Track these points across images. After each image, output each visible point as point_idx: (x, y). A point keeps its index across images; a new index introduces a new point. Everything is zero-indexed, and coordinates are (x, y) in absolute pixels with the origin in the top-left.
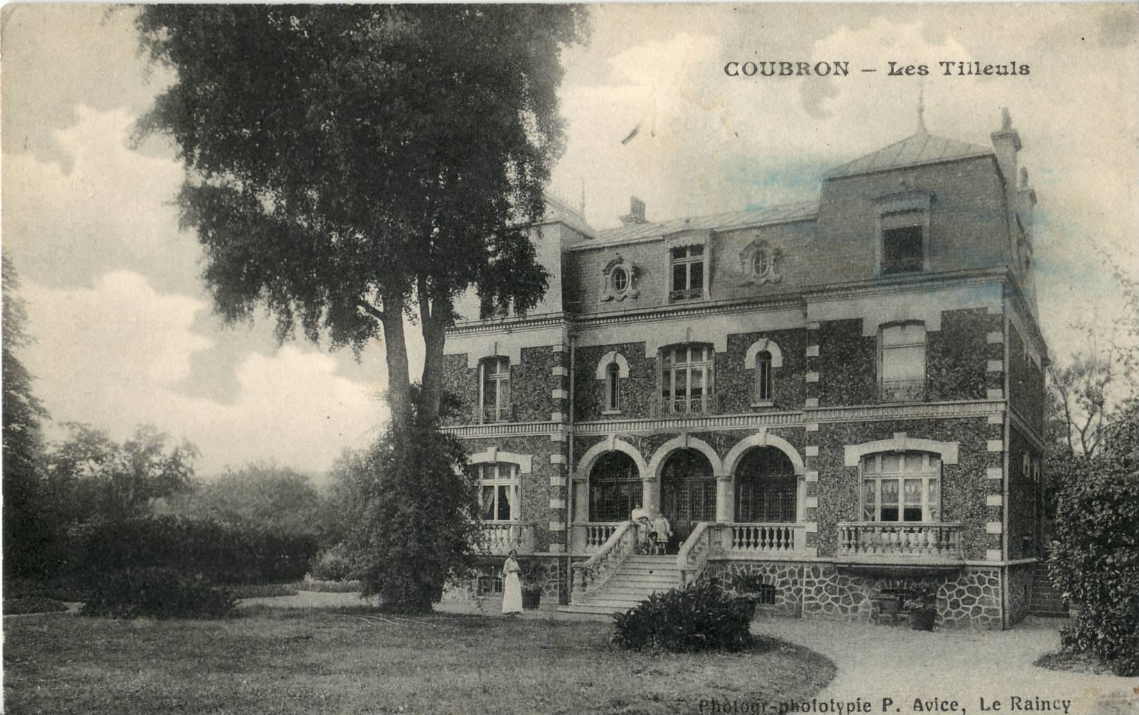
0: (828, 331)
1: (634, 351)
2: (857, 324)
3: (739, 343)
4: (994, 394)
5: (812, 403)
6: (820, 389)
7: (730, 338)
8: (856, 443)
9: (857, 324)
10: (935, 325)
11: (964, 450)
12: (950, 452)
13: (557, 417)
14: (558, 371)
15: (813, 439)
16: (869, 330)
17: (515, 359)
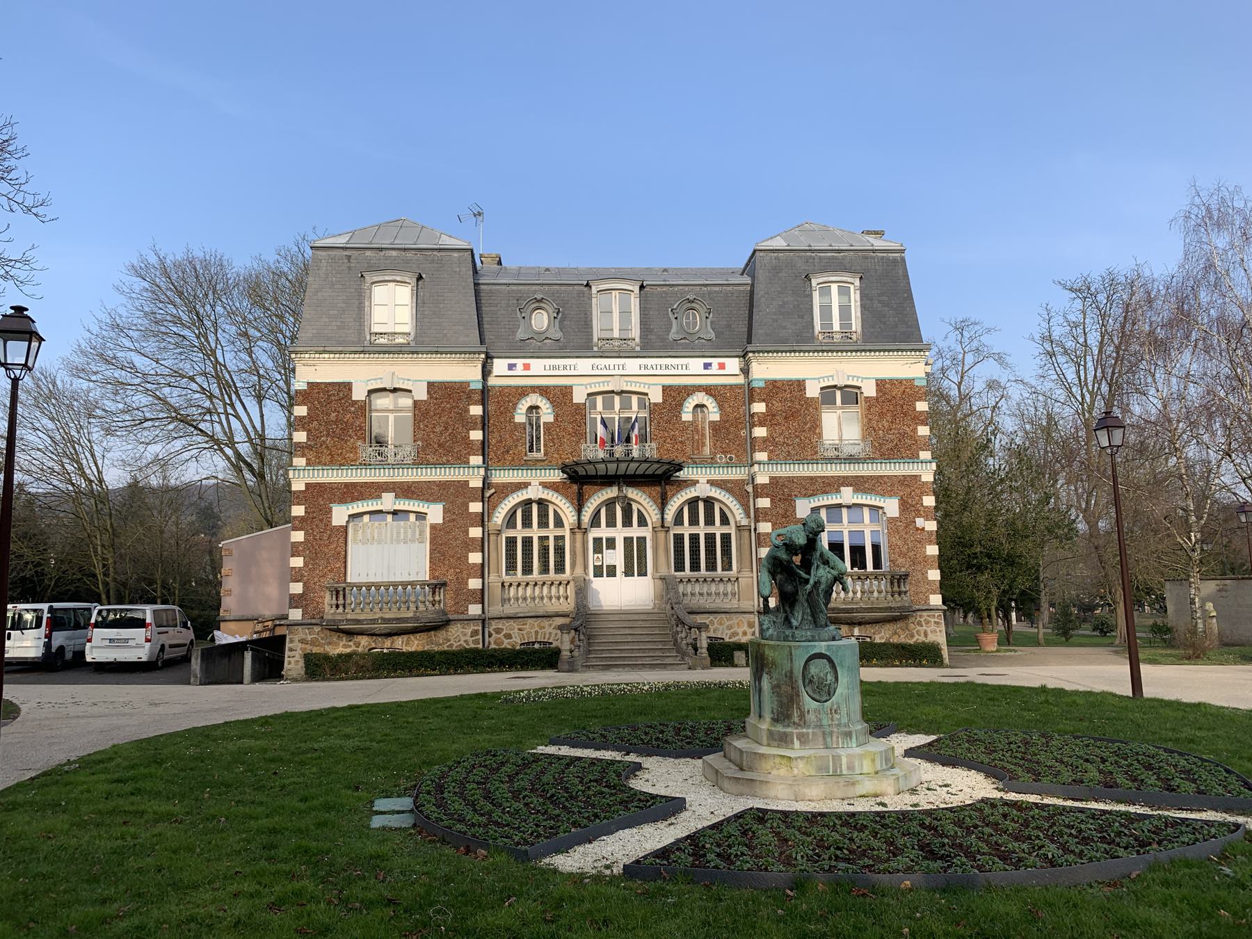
0: (774, 389)
1: (559, 396)
2: (800, 385)
3: (676, 395)
4: (925, 455)
5: (762, 456)
6: (765, 443)
7: (666, 389)
8: (805, 496)
9: (800, 385)
10: (870, 390)
11: (904, 506)
12: (892, 507)
13: (476, 460)
14: (476, 410)
15: (759, 491)
16: (812, 391)
17: (421, 394)
